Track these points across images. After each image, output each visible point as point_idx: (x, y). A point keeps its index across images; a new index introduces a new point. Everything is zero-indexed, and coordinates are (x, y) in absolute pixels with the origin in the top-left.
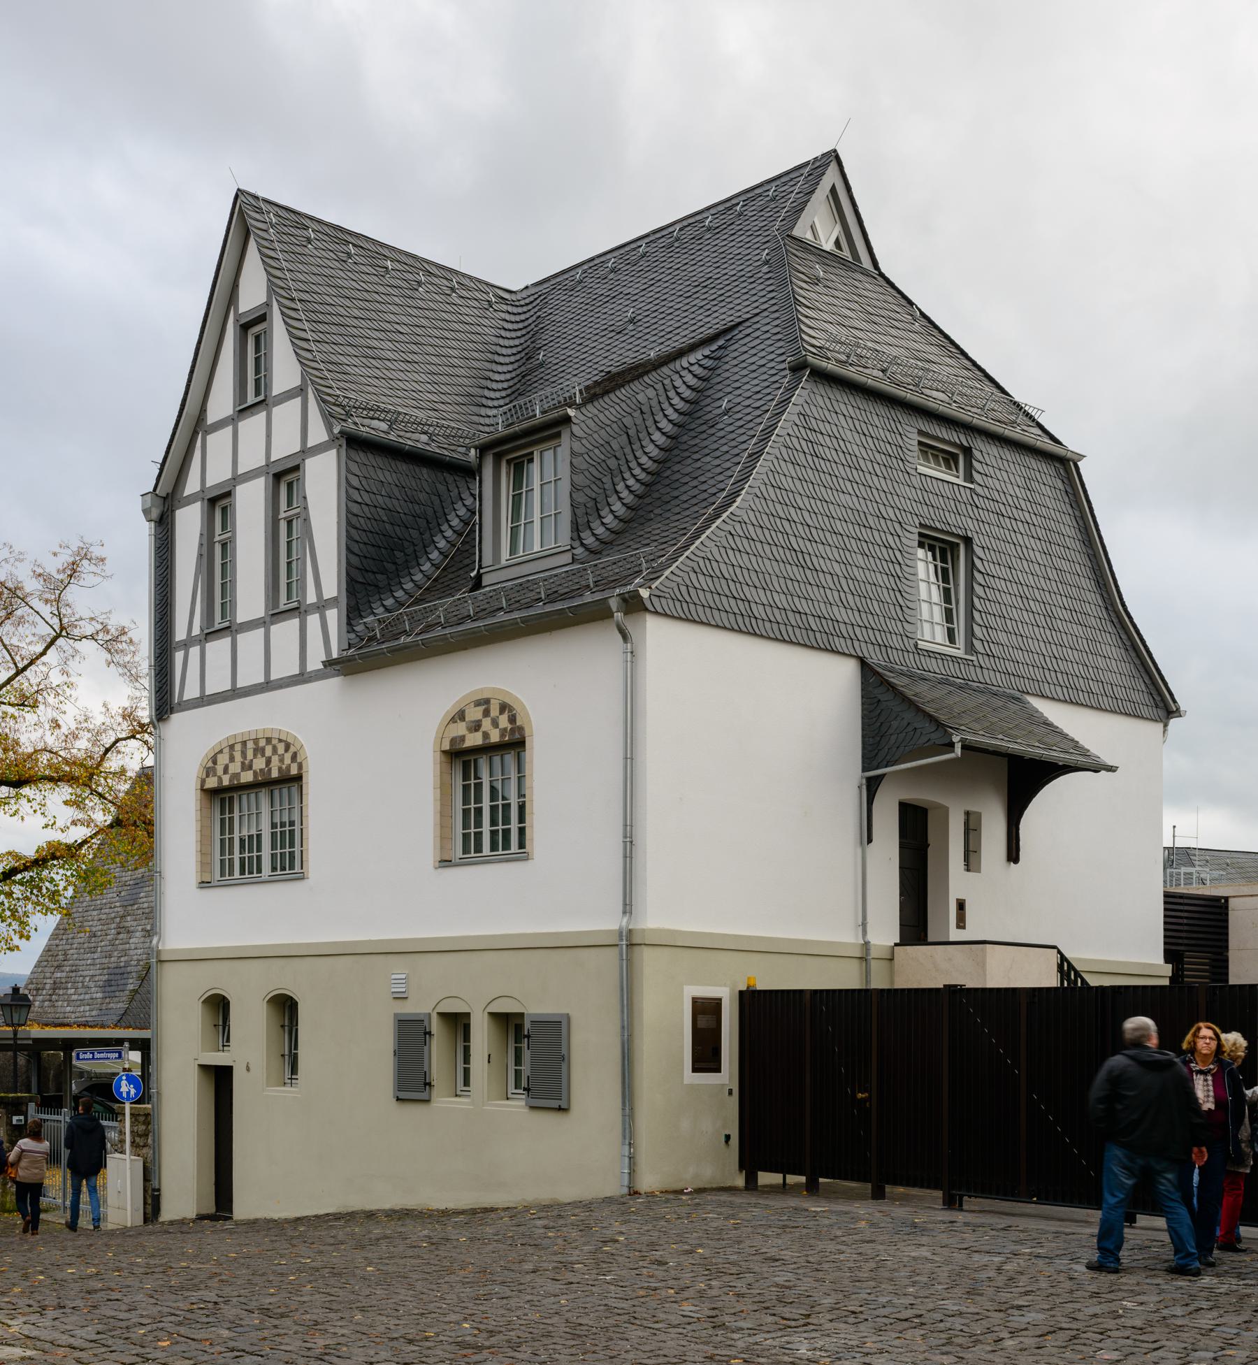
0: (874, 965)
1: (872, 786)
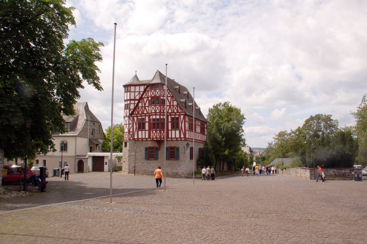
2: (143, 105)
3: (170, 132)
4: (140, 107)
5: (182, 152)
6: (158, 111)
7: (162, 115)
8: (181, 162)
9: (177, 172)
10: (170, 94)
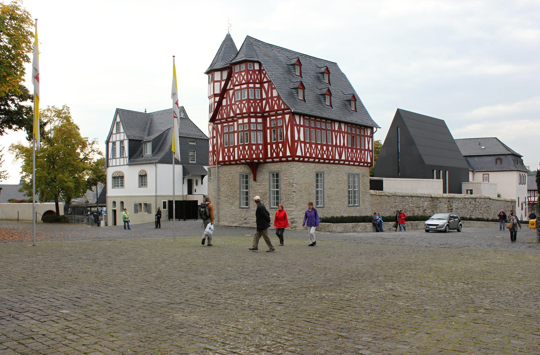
0: (184, 197)
1: (184, 178)
2: (229, 103)
4: (225, 106)
6: (244, 111)
7: (253, 117)
10: (267, 78)
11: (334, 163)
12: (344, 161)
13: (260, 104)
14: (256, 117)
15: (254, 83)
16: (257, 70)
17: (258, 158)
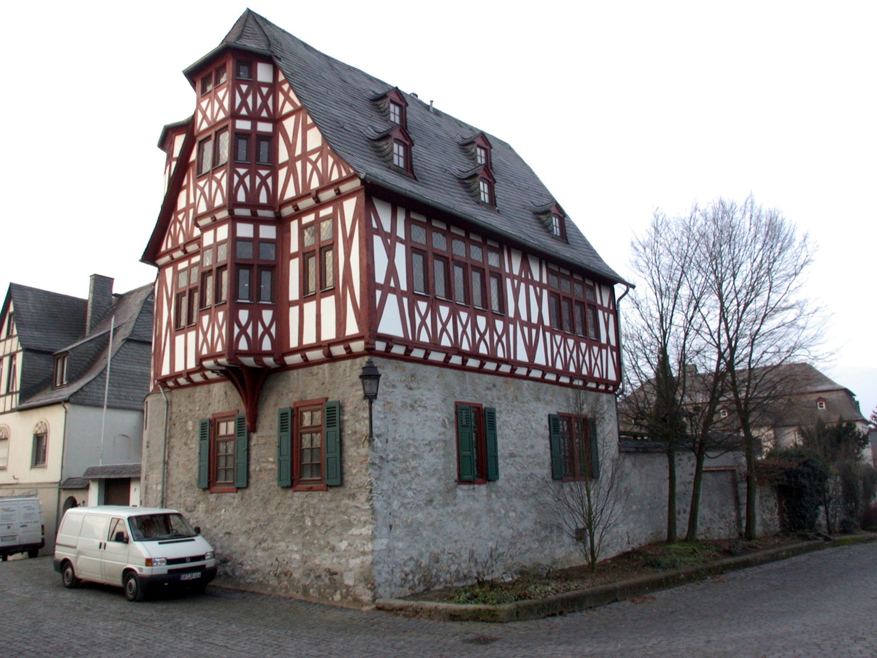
3: (294, 312)
5: (355, 433)
7: (244, 220)
8: (351, 503)
9: (336, 568)
10: (292, 103)
11: (512, 374)
12: (545, 369)
13: (269, 181)
14: (256, 221)
15: (254, 117)
16: (265, 84)
17: (255, 350)
